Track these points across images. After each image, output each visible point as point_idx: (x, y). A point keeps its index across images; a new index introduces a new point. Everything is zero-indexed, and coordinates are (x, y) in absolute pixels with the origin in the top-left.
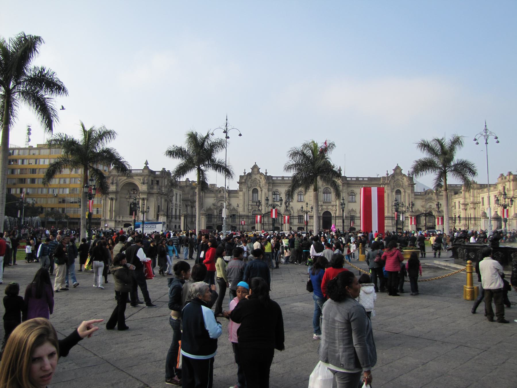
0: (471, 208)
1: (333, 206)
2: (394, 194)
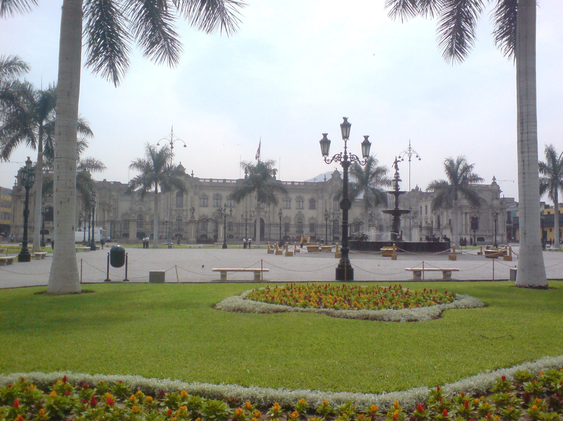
1: (266, 212)
2: (332, 200)
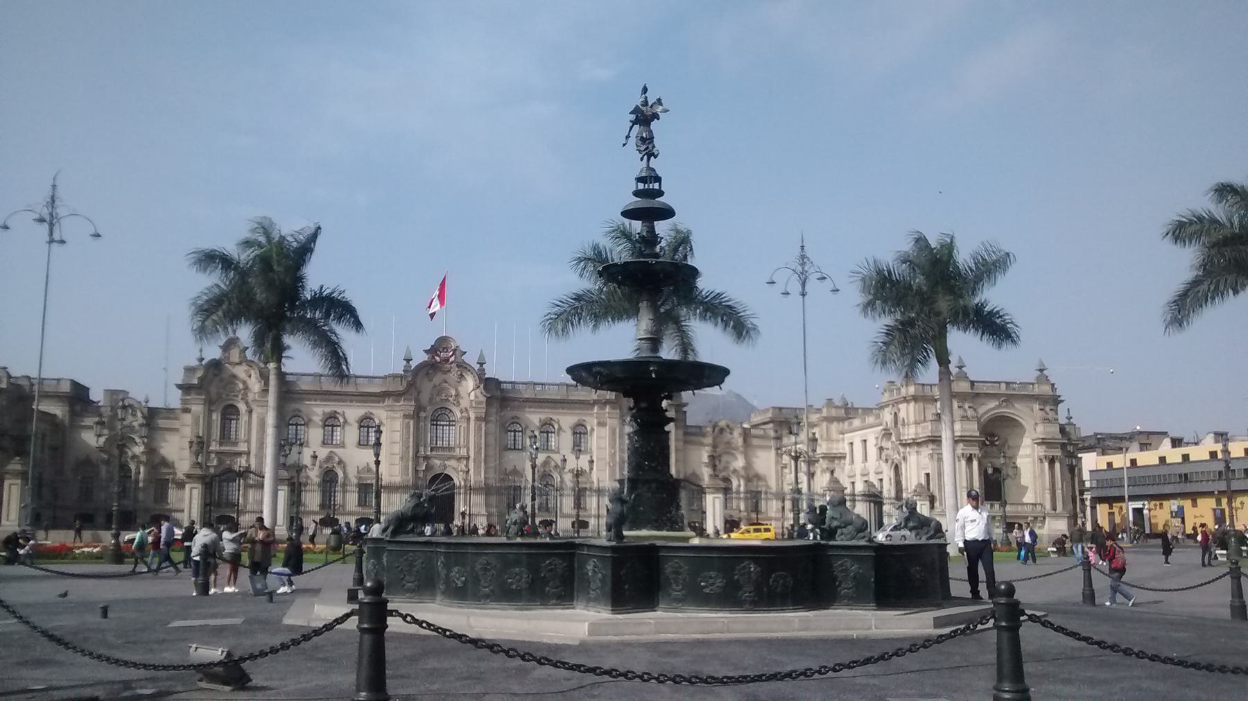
0: (823, 471)
